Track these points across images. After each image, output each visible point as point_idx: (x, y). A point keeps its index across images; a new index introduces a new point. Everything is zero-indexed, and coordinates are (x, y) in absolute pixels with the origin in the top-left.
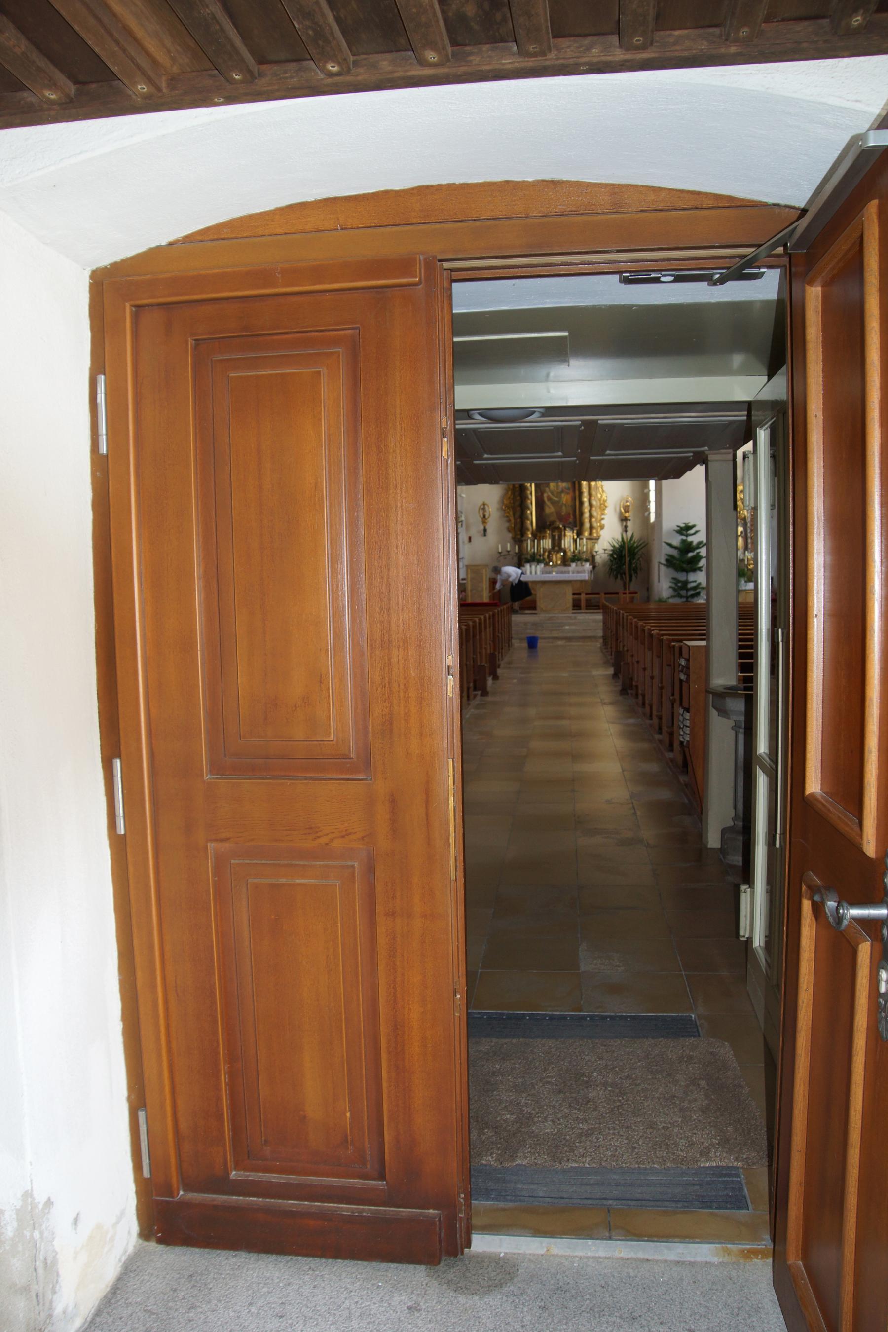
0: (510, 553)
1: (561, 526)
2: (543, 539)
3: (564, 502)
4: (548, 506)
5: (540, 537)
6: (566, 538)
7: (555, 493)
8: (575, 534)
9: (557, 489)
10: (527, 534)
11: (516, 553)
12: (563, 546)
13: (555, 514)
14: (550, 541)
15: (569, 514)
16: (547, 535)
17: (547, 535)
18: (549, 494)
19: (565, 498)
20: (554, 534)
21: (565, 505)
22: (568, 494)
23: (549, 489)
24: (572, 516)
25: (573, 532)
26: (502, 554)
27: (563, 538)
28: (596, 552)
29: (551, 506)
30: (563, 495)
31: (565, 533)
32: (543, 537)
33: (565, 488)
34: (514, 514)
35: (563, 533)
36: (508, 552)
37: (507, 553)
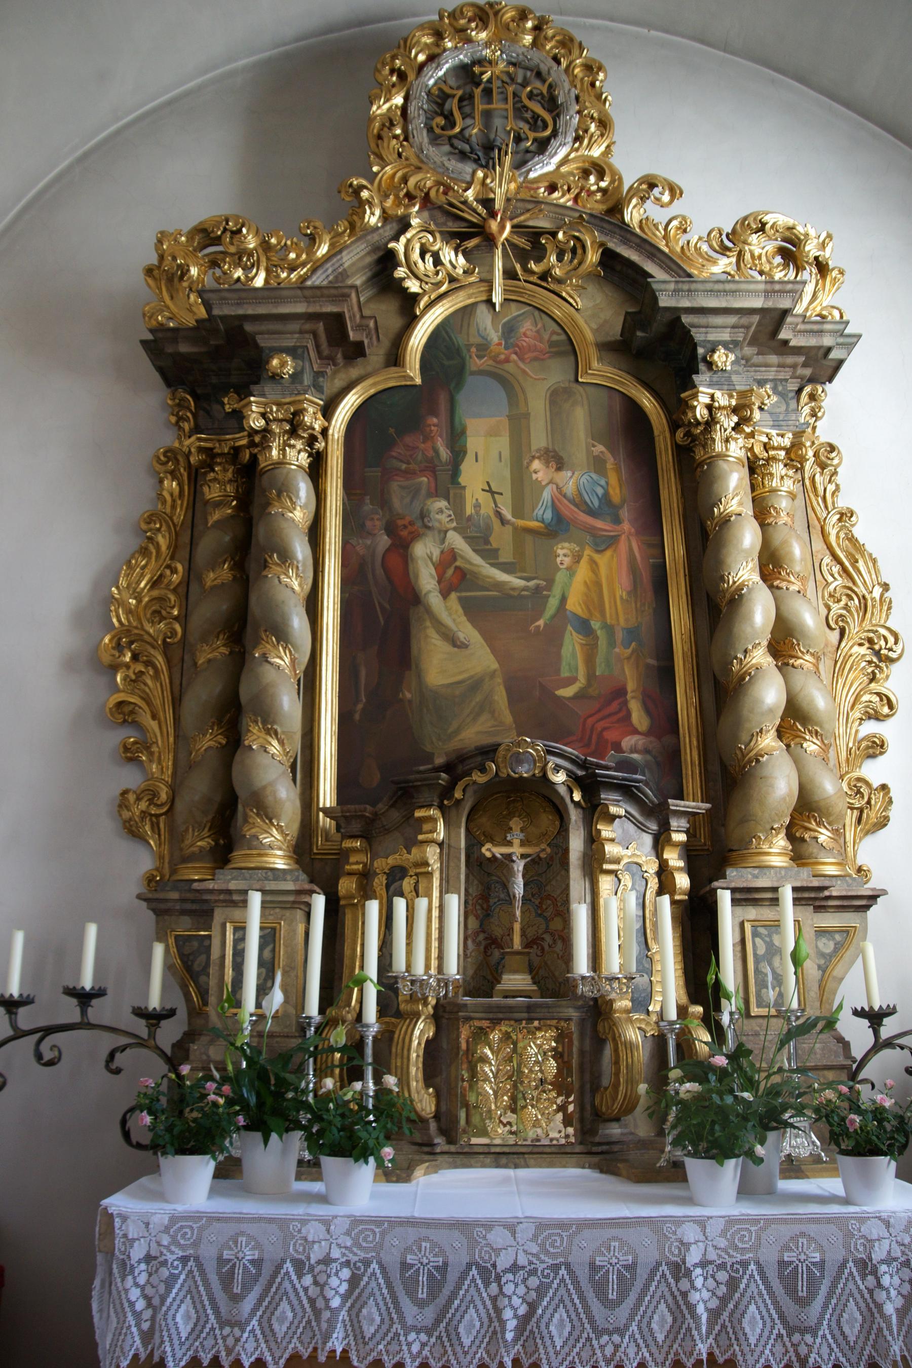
0: (99, 1011)
1: (560, 778)
2: (393, 889)
3: (574, 605)
4: (438, 625)
5: (365, 877)
6: (606, 883)
7: (502, 539)
8: (674, 859)
9: (518, 512)
10: (254, 844)
11: (154, 1018)
12: (582, 965)
13: (501, 697)
14: (454, 903)
15: (620, 692)
16: (432, 854)
17: (432, 854)
18: (456, 540)
19: (583, 572)
20: (489, 850)
21: (584, 627)
22: (603, 543)
23: (457, 505)
24: (638, 717)
25: (660, 842)
26: (26, 1018)
27: (577, 884)
28: (875, 1018)
29: (467, 631)
30: (563, 552)
31: (593, 841)
32: (396, 874)
33: (580, 503)
34: (177, 702)
35: (576, 844)
36: (84, 998)
37: (70, 1011)
